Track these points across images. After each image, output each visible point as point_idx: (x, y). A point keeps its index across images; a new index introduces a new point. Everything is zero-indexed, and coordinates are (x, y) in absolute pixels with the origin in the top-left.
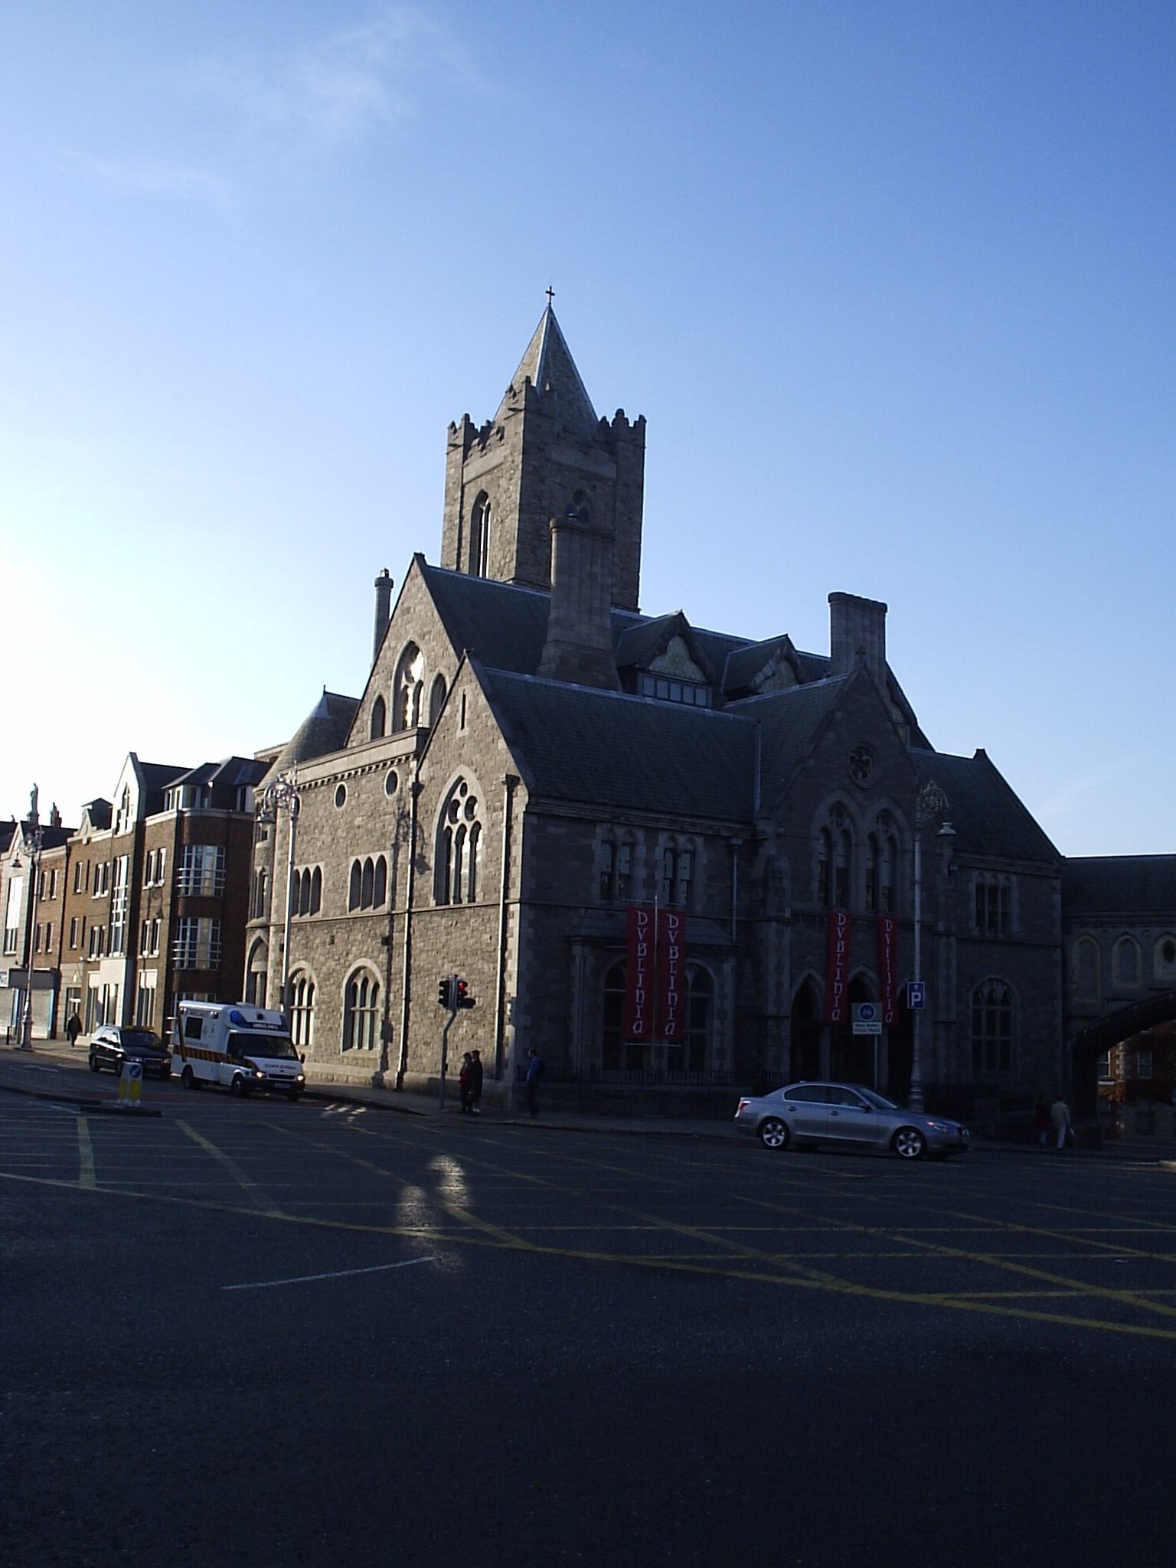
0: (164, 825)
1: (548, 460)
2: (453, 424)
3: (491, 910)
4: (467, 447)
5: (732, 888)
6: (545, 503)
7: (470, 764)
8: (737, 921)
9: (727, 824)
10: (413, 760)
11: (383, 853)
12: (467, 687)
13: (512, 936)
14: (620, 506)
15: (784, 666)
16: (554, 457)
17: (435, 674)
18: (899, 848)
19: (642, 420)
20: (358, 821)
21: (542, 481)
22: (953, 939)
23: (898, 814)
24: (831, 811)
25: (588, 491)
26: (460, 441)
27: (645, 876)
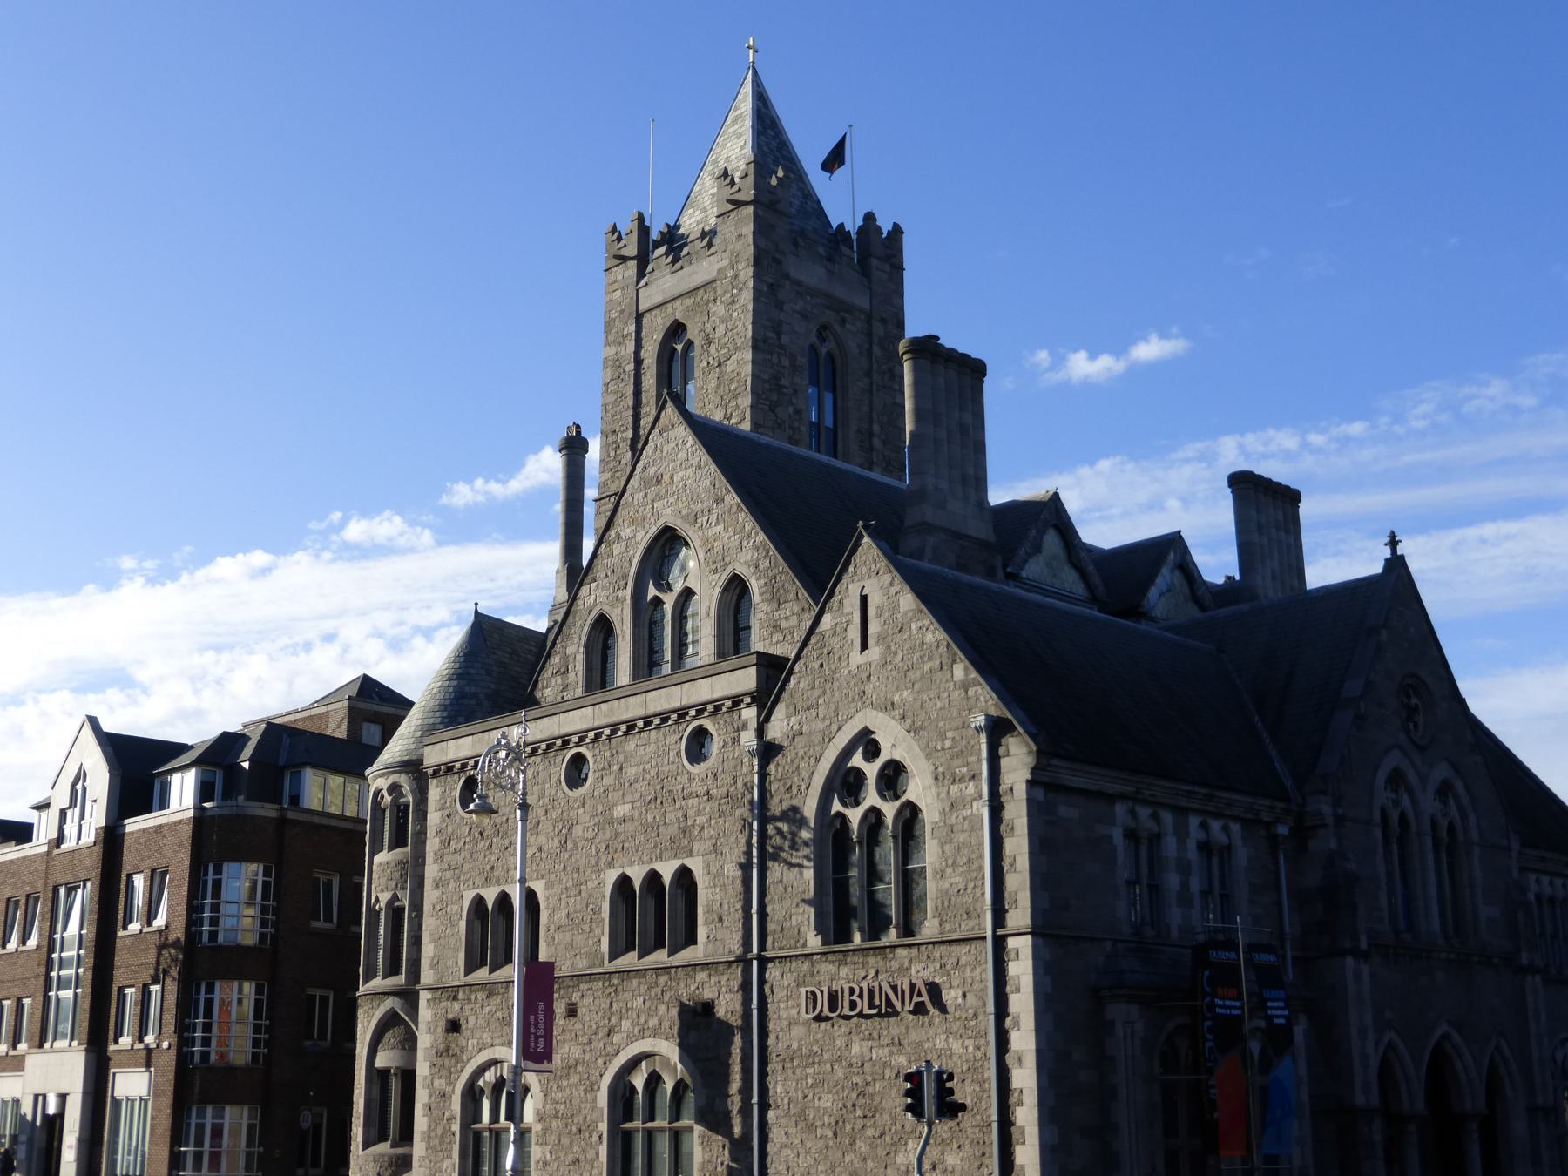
0: (165, 831)
1: (787, 276)
2: (614, 229)
3: (978, 944)
4: (643, 260)
5: (1279, 904)
6: (785, 339)
7: (888, 706)
8: (1293, 957)
9: (1268, 802)
10: (749, 705)
11: (689, 863)
12: (867, 583)
13: (1018, 990)
14: (877, 351)
15: (1178, 578)
16: (793, 273)
17: (725, 576)
18: (1461, 838)
19: (897, 231)
20: (621, 811)
21: (779, 305)
22: (1538, 978)
23: (1459, 786)
24: (1386, 783)
25: (837, 327)
26: (631, 250)
27: (1178, 888)
